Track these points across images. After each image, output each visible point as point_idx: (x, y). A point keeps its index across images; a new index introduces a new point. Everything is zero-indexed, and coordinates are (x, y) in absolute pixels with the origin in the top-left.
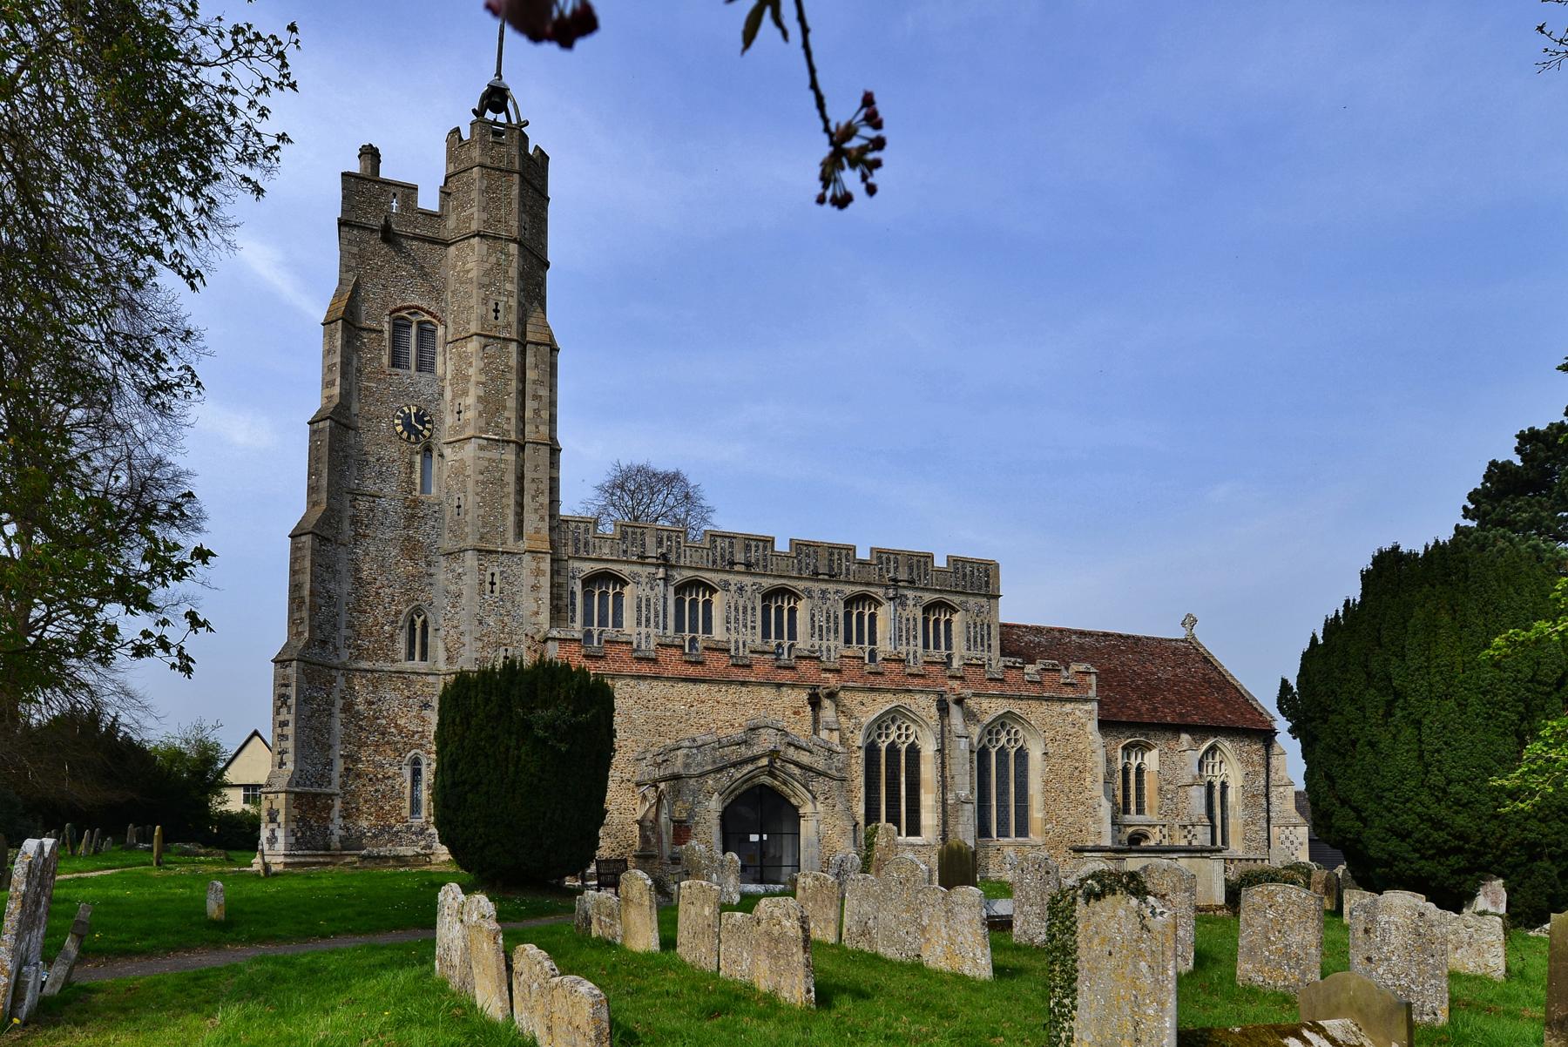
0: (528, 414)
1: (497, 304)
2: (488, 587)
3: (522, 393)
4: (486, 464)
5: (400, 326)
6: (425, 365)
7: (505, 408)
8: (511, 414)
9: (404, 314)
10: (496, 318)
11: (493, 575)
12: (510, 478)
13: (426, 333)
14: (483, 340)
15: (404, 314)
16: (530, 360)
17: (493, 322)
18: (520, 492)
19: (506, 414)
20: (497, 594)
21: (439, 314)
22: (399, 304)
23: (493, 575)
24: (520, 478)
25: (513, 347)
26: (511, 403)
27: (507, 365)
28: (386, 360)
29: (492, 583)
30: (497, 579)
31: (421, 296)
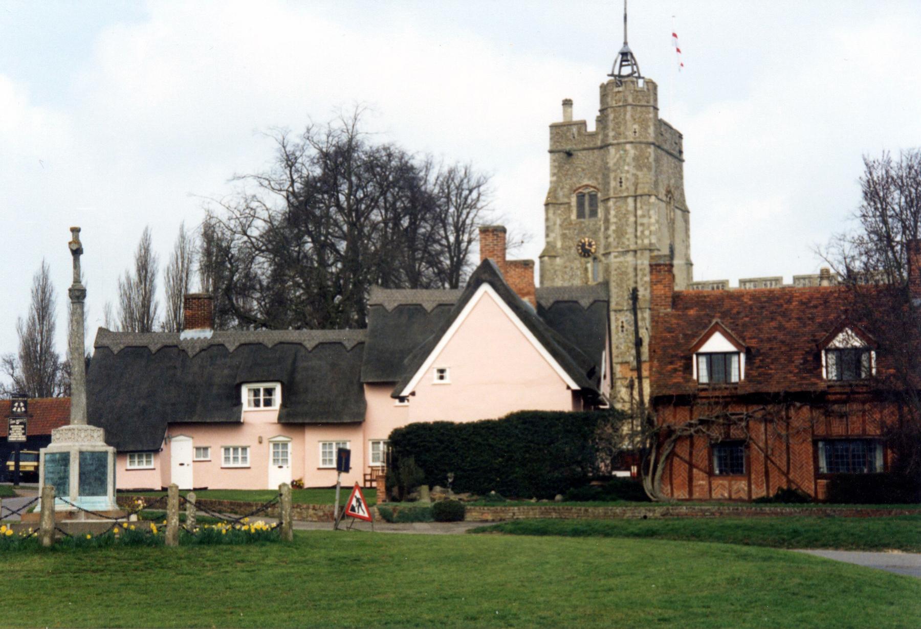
0: (639, 234)
1: (621, 179)
2: (620, 329)
3: (636, 222)
4: (618, 265)
5: (581, 197)
6: (594, 213)
7: (626, 233)
8: (630, 235)
9: (580, 190)
10: (621, 186)
11: (622, 322)
12: (631, 270)
13: (593, 197)
14: (614, 200)
15: (580, 190)
16: (639, 205)
17: (619, 188)
18: (636, 275)
19: (627, 236)
20: (625, 332)
21: (598, 187)
22: (578, 185)
23: (622, 322)
24: (636, 269)
25: (630, 201)
26: (630, 230)
27: (627, 210)
28: (574, 216)
29: (622, 327)
30: (625, 325)
31: (589, 179)
